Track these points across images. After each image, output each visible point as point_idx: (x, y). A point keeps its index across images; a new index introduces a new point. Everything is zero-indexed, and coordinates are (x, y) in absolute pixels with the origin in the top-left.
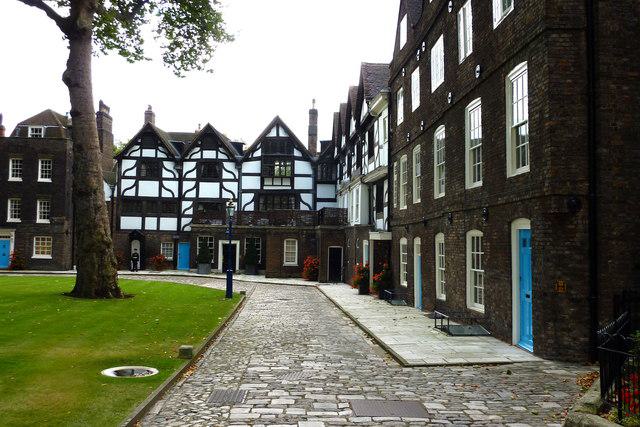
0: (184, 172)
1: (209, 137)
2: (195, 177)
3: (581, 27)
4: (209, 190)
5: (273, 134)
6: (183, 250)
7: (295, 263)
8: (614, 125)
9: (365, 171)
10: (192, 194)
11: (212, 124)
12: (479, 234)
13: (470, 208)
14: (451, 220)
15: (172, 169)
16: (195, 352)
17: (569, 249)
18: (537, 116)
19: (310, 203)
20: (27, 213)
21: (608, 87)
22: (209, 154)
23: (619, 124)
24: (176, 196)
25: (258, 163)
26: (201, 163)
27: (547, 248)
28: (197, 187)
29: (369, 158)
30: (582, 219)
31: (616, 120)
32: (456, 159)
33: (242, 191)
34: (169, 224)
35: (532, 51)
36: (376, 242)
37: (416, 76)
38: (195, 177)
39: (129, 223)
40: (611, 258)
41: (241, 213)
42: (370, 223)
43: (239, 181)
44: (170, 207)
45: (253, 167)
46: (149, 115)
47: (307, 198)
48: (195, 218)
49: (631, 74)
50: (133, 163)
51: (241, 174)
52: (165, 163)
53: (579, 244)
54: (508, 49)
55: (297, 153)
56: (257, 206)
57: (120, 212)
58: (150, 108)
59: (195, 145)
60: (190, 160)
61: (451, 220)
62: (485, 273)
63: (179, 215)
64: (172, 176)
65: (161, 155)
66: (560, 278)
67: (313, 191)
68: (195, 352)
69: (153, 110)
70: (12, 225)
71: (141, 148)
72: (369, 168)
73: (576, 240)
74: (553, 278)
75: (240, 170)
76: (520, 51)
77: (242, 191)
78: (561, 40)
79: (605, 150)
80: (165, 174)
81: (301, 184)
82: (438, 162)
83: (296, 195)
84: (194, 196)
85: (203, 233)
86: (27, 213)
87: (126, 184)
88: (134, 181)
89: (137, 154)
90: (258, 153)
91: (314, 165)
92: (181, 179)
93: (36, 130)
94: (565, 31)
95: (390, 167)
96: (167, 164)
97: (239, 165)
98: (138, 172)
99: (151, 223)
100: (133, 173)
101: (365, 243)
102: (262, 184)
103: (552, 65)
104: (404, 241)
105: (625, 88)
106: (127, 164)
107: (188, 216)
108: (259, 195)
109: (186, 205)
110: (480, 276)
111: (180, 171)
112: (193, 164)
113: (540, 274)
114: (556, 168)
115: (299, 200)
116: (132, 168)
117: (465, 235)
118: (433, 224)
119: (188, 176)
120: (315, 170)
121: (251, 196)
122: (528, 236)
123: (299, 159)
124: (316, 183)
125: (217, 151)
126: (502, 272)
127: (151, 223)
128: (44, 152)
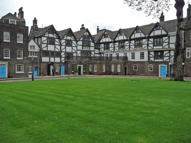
0: (62, 43)
1: (69, 32)
4: (69, 49)
5: (85, 34)
6: (63, 68)
10: (64, 50)
15: (58, 41)
19: (93, 54)
20: (13, 55)
22: (69, 38)
24: (60, 51)
28: (65, 48)
38: (65, 45)
39: (45, 59)
41: (77, 56)
43: (77, 47)
44: (58, 54)
45: (80, 43)
47: (93, 53)
52: (56, 39)
56: (81, 55)
58: (35, 18)
59: (65, 35)
63: (61, 57)
64: (58, 44)
65: (55, 37)
67: (94, 51)
71: (48, 33)
77: (77, 50)
80: (56, 43)
81: (92, 49)
85: (73, 63)
86: (13, 55)
87: (43, 46)
89: (47, 35)
90: (82, 39)
92: (61, 45)
96: (56, 39)
97: (77, 41)
98: (47, 42)
99: (52, 60)
100: (46, 42)
102: (83, 48)
106: (44, 39)
107: (63, 57)
108: (82, 52)
109: (62, 54)
111: (60, 43)
112: (64, 41)
115: (91, 53)
116: (45, 40)
120: (95, 45)
121: (80, 51)
124: (95, 49)
125: (71, 37)
127: (52, 60)
128: (20, 31)
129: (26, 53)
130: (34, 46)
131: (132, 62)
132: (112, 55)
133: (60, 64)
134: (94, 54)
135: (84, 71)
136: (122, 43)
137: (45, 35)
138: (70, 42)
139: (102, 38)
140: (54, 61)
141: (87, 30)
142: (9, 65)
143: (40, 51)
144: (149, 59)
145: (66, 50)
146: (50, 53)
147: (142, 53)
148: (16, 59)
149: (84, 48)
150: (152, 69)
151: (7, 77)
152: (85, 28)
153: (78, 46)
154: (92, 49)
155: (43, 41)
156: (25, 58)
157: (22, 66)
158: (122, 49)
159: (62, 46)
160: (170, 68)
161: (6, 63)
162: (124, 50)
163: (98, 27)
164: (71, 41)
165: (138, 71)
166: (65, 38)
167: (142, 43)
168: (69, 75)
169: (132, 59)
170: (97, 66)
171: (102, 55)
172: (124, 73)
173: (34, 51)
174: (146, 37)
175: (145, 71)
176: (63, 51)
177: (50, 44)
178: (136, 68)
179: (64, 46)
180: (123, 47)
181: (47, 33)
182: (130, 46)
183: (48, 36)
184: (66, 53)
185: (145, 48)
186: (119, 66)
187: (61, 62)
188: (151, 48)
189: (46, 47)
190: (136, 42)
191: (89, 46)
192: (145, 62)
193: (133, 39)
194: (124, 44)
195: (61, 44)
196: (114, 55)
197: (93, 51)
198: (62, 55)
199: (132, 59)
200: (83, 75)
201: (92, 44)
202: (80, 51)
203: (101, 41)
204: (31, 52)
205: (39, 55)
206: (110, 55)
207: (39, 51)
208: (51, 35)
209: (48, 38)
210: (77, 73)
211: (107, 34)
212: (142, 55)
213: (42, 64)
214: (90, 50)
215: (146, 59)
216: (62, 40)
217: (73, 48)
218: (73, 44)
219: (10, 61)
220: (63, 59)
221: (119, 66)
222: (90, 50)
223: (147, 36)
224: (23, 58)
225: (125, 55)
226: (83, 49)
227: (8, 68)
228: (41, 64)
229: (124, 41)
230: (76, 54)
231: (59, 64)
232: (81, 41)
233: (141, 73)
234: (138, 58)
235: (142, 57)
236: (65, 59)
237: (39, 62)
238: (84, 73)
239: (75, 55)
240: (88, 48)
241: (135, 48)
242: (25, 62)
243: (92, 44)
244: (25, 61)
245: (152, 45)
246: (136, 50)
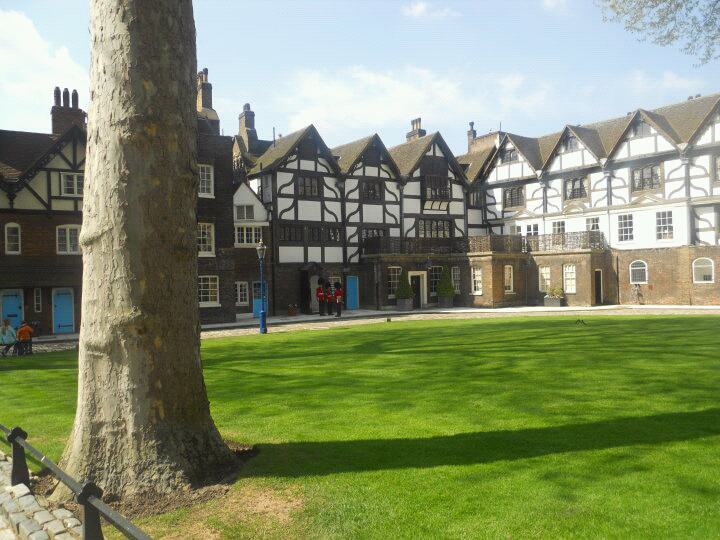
0: (346, 192)
1: (374, 151)
2: (357, 197)
4: (373, 214)
5: (430, 153)
6: (353, 285)
10: (355, 219)
22: (372, 171)
24: (340, 220)
28: (360, 209)
33: (403, 216)
34: (334, 255)
38: (357, 197)
39: (290, 254)
41: (403, 239)
43: (400, 203)
45: (413, 188)
47: (460, 223)
50: (291, 176)
56: (417, 233)
58: (247, 106)
60: (352, 177)
65: (321, 169)
67: (464, 217)
69: (252, 109)
71: (299, 159)
77: (403, 216)
80: (327, 193)
81: (457, 208)
83: (450, 220)
84: (358, 221)
87: (283, 203)
88: (290, 201)
89: (293, 166)
90: (417, 174)
92: (343, 200)
97: (401, 182)
99: (314, 254)
100: (290, 190)
102: (422, 208)
106: (283, 178)
107: (354, 245)
109: (351, 231)
111: (342, 191)
115: (452, 226)
119: (351, 196)
120: (467, 195)
121: (413, 220)
124: (468, 206)
125: (380, 168)
127: (314, 254)
129: (225, 235)
130: (250, 208)
131: (620, 251)
132: (536, 228)
133: (345, 270)
134: (463, 229)
135: (433, 294)
136: (576, 180)
139: (493, 166)
140: (320, 261)
141: (438, 140)
144: (694, 239)
147: (664, 214)
149: (428, 205)
150: (707, 278)
152: (422, 133)
153: (405, 200)
154: (457, 208)
155: (281, 188)
157: (214, 280)
158: (577, 202)
159: (348, 205)
162: (584, 207)
163: (472, 124)
164: (380, 182)
165: (650, 287)
166: (359, 173)
167: (663, 174)
168: (378, 309)
169: (621, 239)
170: (483, 273)
171: (497, 231)
172: (589, 293)
173: (250, 225)
174: (677, 150)
175: (680, 286)
177: (305, 197)
178: (639, 275)
179: (354, 201)
180: (580, 193)
181: (295, 157)
182: (609, 190)
184: (362, 226)
185: (674, 196)
186: (570, 272)
187: (346, 262)
188: (701, 194)
190: (637, 176)
191: (446, 197)
192: (680, 248)
193: (703, 151)
194: (585, 184)
196: (546, 228)
198: (348, 236)
199: (621, 239)
200: (429, 308)
201: (457, 191)
202: (413, 220)
203: (491, 179)
204: (241, 229)
205: (269, 240)
206: (529, 228)
207: (267, 224)
208: (308, 165)
209: (299, 174)
210: (409, 302)
211: (512, 151)
212: (664, 223)
214: (452, 212)
215: (680, 237)
216: (348, 181)
220: (351, 250)
221: (570, 272)
223: (683, 146)
224: (217, 253)
225: (591, 225)
226: (425, 212)
228: (276, 269)
229: (585, 172)
230: (398, 230)
232: (416, 180)
233: (663, 295)
234: (645, 236)
235: (665, 228)
236: (359, 252)
238: (430, 299)
239: (394, 233)
240: (444, 205)
241: (631, 195)
243: (457, 191)
245: (705, 183)
246: (635, 204)
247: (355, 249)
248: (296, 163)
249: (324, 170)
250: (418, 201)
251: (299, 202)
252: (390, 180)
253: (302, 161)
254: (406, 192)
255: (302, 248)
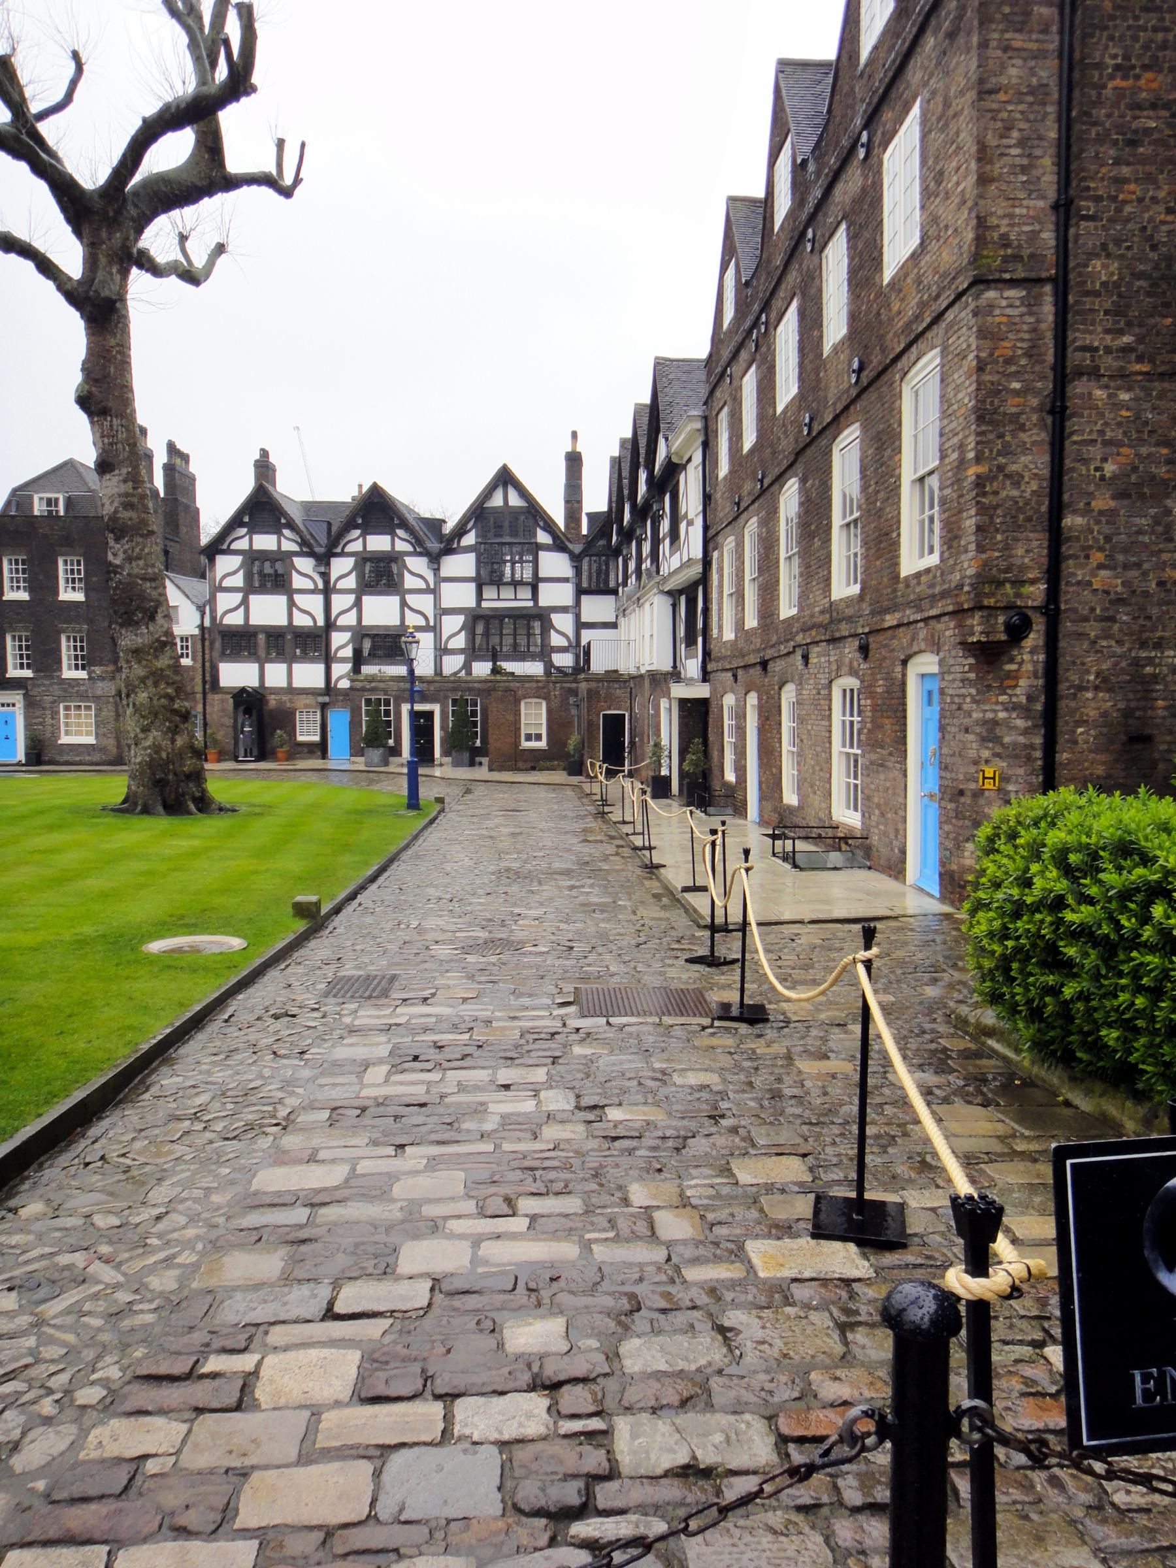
3: (1044, 275)
5: (497, 501)
6: (339, 721)
7: (542, 744)
8: (1096, 469)
9: (665, 570)
10: (350, 619)
11: (380, 484)
12: (852, 682)
13: (837, 635)
14: (806, 658)
15: (310, 572)
16: (324, 910)
17: (1006, 710)
18: (955, 456)
21: (1090, 394)
22: (379, 543)
23: (1110, 468)
24: (321, 622)
25: (471, 558)
26: (364, 559)
27: (965, 707)
28: (358, 604)
29: (672, 543)
30: (1032, 652)
31: (1104, 460)
32: (817, 543)
35: (951, 325)
36: (683, 702)
37: (749, 383)
40: (1080, 723)
42: (675, 667)
43: (435, 592)
45: (462, 564)
46: (264, 468)
47: (563, 622)
48: (358, 660)
49: (1138, 367)
50: (235, 561)
51: (440, 580)
53: (1023, 699)
54: (908, 325)
55: (543, 537)
57: (216, 654)
58: (264, 453)
60: (343, 554)
61: (806, 658)
62: (863, 756)
63: (328, 660)
64: (311, 586)
65: (288, 546)
66: (987, 762)
68: (324, 910)
70: (18, 684)
71: (251, 532)
72: (671, 562)
73: (1018, 691)
74: (976, 763)
75: (436, 571)
76: (929, 327)
78: (1004, 303)
79: (1079, 520)
80: (298, 582)
81: (555, 595)
82: (786, 546)
83: (542, 616)
84: (354, 622)
87: (225, 601)
89: (242, 545)
91: (576, 559)
92: (327, 591)
93: (49, 502)
94: (1013, 283)
95: (707, 562)
97: (435, 560)
99: (276, 675)
100: (238, 580)
101: (664, 703)
102: (480, 597)
103: (983, 355)
104: (729, 700)
105: (1124, 396)
106: (226, 564)
107: (343, 660)
109: (339, 640)
110: (856, 761)
111: (325, 576)
113: (953, 755)
114: (984, 556)
115: (547, 626)
116: (235, 573)
117: (829, 686)
118: (776, 667)
119: (340, 585)
120: (578, 571)
122: (934, 686)
123: (546, 548)
124: (580, 592)
125: (393, 535)
126: (891, 754)
127: (276, 675)
133: (321, 699)
134: (569, 630)
137: (234, 546)
138: (395, 570)
142: (31, 704)
143: (202, 627)
145: (360, 619)
146: (261, 637)
148: (59, 677)
151: (21, 756)
154: (555, 595)
156: (98, 670)
157: (88, 708)
159: (335, 598)
160: (762, 730)
161: (17, 697)
176: (341, 621)
177: (262, 590)
181: (244, 531)
183: (246, 547)
184: (360, 633)
187: (329, 689)
189: (242, 609)
195: (327, 582)
197: (564, 610)
198: (334, 648)
201: (555, 564)
207: (196, 632)
213: (217, 697)
214: (542, 603)
217: (409, 598)
218: (406, 574)
219: (34, 686)
220: (340, 670)
222: (542, 603)
226: (484, 604)
227: (26, 717)
228: (210, 696)
231: (310, 700)
232: (468, 549)
236: (356, 669)
237: (199, 688)
242: (99, 693)
244: (100, 684)
247: (348, 667)
248: (247, 538)
249: (295, 547)
250: (472, 586)
251: (254, 599)
252: (415, 554)
253: (255, 537)
254: (444, 573)
255: (256, 666)
